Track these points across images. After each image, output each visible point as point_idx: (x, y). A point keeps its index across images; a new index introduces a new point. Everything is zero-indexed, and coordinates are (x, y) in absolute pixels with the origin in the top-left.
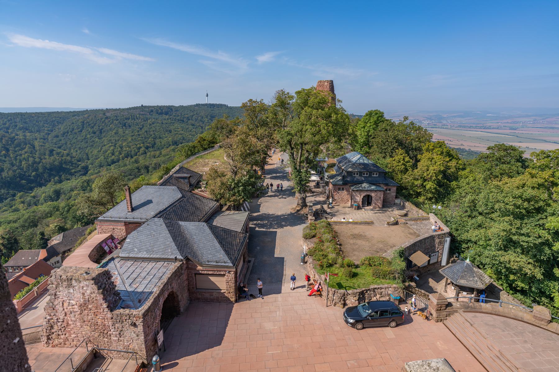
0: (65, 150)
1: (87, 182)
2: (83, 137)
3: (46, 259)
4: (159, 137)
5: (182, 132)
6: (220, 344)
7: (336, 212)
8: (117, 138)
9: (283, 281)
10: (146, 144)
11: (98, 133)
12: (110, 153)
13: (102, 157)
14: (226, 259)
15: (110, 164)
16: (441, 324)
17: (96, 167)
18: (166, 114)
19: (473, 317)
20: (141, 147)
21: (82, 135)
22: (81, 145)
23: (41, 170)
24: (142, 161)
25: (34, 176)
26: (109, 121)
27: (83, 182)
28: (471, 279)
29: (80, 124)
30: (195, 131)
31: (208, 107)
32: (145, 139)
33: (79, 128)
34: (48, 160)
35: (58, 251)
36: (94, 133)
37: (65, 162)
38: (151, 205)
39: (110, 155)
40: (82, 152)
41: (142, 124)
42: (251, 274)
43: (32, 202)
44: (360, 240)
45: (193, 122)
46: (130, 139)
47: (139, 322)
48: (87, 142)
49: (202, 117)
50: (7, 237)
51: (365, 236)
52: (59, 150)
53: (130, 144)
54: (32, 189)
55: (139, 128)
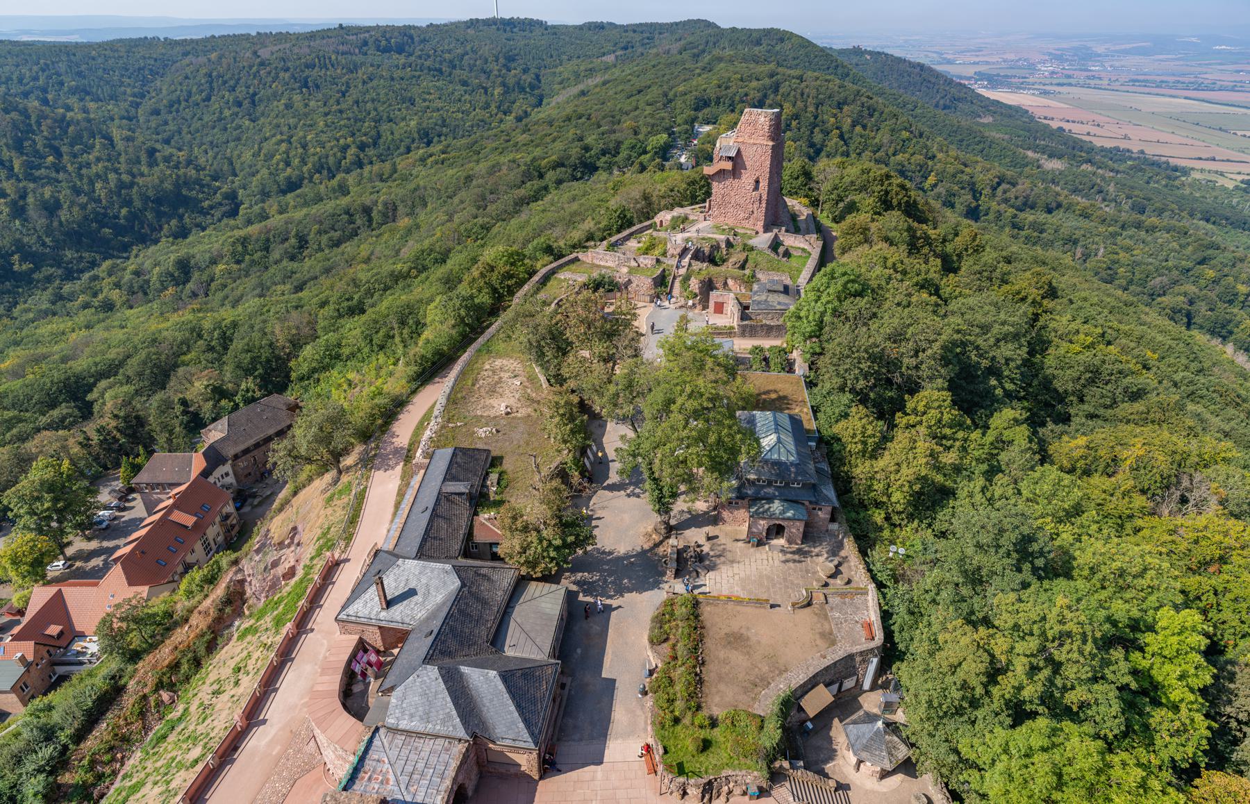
0: (180, 150)
1: (243, 244)
3: (205, 473)
5: (438, 104)
7: (719, 556)
11: (246, 104)
13: (265, 172)
14: (525, 735)
18: (400, 50)
20: (348, 146)
21: (211, 109)
23: (138, 203)
24: (358, 195)
25: (125, 218)
26: (269, 73)
31: (498, 29)
33: (202, 91)
34: (152, 178)
35: (224, 454)
36: (240, 104)
37: (185, 183)
38: (416, 598)
39: (281, 165)
40: (217, 154)
41: (344, 80)
43: (135, 285)
45: (464, 75)
46: (322, 123)
48: (225, 129)
49: (486, 61)
50: (122, 414)
51: (748, 639)
52: (168, 150)
53: (324, 137)
54: (126, 248)
55: (338, 92)
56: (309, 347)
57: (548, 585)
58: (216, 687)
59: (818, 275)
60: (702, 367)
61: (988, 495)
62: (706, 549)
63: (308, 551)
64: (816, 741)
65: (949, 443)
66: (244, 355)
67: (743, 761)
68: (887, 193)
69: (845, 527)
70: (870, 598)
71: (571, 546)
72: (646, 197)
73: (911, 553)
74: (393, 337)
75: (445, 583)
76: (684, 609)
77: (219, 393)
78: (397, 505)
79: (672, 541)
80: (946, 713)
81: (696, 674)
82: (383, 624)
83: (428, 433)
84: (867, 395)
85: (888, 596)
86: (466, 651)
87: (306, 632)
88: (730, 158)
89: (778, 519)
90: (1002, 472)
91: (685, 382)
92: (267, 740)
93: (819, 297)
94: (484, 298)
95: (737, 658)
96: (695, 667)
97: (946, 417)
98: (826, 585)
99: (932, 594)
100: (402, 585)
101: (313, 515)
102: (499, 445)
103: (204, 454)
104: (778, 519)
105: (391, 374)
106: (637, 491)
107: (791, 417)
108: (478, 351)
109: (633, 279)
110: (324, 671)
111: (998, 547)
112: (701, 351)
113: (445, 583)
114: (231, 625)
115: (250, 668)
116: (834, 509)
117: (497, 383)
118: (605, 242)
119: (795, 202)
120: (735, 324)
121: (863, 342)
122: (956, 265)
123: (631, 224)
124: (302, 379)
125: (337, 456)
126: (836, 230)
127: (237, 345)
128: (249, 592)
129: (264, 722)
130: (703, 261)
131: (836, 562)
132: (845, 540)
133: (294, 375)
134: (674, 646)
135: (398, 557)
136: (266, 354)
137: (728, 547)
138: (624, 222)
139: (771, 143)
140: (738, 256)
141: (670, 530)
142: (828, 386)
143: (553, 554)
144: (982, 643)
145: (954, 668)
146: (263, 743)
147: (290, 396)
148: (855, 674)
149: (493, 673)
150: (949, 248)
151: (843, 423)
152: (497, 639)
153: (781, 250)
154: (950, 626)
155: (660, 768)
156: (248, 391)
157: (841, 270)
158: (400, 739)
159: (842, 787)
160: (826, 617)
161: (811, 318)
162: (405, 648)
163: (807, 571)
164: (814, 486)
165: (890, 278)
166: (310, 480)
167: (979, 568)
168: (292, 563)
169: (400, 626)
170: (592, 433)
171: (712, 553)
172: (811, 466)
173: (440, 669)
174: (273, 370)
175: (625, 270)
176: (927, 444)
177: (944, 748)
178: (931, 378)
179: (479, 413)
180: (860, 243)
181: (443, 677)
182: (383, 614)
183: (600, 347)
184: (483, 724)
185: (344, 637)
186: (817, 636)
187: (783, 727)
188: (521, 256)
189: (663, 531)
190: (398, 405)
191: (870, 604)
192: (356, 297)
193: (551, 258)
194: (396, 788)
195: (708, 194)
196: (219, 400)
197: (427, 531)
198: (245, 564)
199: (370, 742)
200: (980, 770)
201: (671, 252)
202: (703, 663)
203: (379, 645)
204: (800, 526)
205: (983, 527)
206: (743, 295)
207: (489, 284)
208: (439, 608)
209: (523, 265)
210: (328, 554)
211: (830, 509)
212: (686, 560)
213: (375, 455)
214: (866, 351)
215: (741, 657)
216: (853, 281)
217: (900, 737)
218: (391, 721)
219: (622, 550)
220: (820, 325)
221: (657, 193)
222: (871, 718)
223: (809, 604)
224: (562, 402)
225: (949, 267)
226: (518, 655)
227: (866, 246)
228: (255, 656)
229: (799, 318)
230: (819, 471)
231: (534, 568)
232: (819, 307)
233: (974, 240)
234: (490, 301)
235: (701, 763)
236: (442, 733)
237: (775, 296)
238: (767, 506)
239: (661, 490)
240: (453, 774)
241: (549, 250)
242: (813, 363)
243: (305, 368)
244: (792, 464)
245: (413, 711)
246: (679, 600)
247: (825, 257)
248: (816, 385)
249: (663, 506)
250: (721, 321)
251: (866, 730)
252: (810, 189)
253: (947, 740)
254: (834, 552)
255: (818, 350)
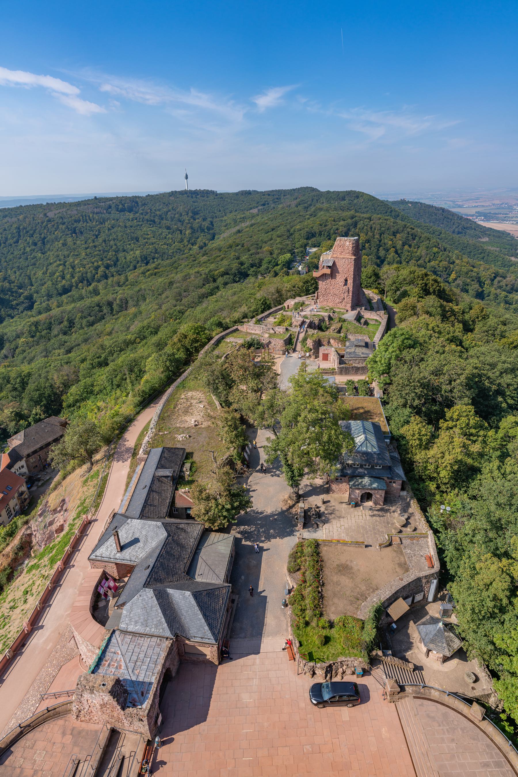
1: (35, 326)
2: (20, 250)
3: (10, 466)
4: (123, 249)
6: (205, 720)
7: (331, 514)
8: (66, 253)
9: (263, 635)
10: (106, 262)
11: (39, 244)
12: (60, 276)
13: (49, 283)
15: (60, 292)
16: (393, 704)
17: (43, 297)
18: (130, 210)
19: (420, 705)
21: (19, 248)
22: (20, 263)
26: (53, 226)
27: (31, 325)
28: (440, 645)
29: (15, 231)
30: (172, 239)
31: (188, 196)
32: (104, 252)
33: (14, 237)
35: (21, 454)
36: (35, 244)
38: (139, 544)
40: (22, 273)
41: (97, 228)
42: (233, 622)
44: (344, 575)
45: (168, 223)
46: (84, 254)
47: (145, 719)
48: (27, 259)
49: (181, 215)
51: (351, 568)
53: (85, 262)
55: (93, 235)
56: (74, 387)
57: (222, 534)
58: (12, 604)
59: (386, 336)
60: (316, 393)
61: (502, 471)
62: (322, 509)
63: (72, 514)
64: (399, 637)
65: (475, 438)
66: (35, 393)
67: (351, 651)
68: (426, 285)
69: (411, 493)
70: (429, 540)
71: (237, 509)
72: (278, 291)
73: (455, 510)
74: (126, 379)
75: (157, 534)
76: (309, 549)
77: (19, 416)
78: (128, 484)
79: (301, 505)
80: (484, 617)
81: (319, 592)
82: (118, 561)
83: (146, 439)
84: (420, 409)
85: (442, 538)
86: (171, 578)
87: (70, 567)
88: (329, 267)
89: (368, 489)
90: (510, 456)
91: (306, 403)
92: (44, 639)
93: (387, 349)
94: (181, 355)
95: (345, 581)
96: (318, 587)
97: (472, 422)
98: (401, 532)
99: (470, 536)
100: (130, 536)
101: (75, 492)
102: (191, 445)
103: (9, 454)
104: (368, 489)
105: (124, 402)
106: (278, 472)
107: (374, 424)
108: (178, 387)
109: (272, 340)
110: (80, 594)
111: (511, 505)
112: (315, 384)
113: (157, 534)
114: (23, 563)
115: (34, 591)
116: (403, 482)
117: (189, 406)
118: (254, 319)
119: (370, 292)
120: (336, 367)
121: (416, 376)
122: (472, 327)
123: (269, 308)
124: (69, 406)
125: (91, 453)
126: (396, 308)
127: (31, 386)
128: (34, 541)
129: (42, 627)
130: (315, 329)
131: (406, 517)
132: (412, 502)
133: (64, 404)
134: (304, 573)
135: (128, 517)
136: (48, 392)
137: (337, 508)
138: (266, 306)
139: (354, 257)
140: (335, 326)
141: (299, 497)
142: (395, 404)
143: (225, 514)
144: (505, 569)
145: (488, 586)
146: (41, 641)
147: (62, 418)
148: (422, 591)
149: (188, 593)
150: (467, 317)
151: (406, 427)
152: (190, 570)
153: (363, 321)
154: (483, 558)
155: (297, 656)
156: (36, 414)
157: (400, 332)
158: (128, 638)
159: (418, 668)
160: (402, 553)
161: (383, 362)
162: (132, 577)
163: (388, 523)
164: (390, 468)
165: (431, 336)
166: (74, 469)
167: (500, 519)
168: (62, 523)
169: (129, 563)
170: (248, 437)
171: (326, 512)
172: (387, 455)
173: (154, 591)
174: (52, 401)
175: (267, 335)
176: (460, 439)
177: (484, 640)
178: (461, 398)
179: (178, 425)
180: (411, 315)
181: (156, 596)
182: (118, 555)
183: (252, 383)
184: (181, 627)
185: (93, 570)
186: (397, 566)
187: (376, 627)
188: (203, 329)
189: (295, 498)
190: (129, 421)
191: (430, 544)
192: (103, 356)
193: (221, 329)
194: (126, 671)
195: (317, 288)
196: (19, 421)
197: (146, 501)
198: (32, 524)
199: (109, 640)
200: (509, 656)
201: (295, 324)
202: (323, 585)
203: (116, 575)
204: (383, 493)
205: (500, 493)
206: (340, 349)
207: (184, 346)
208: (153, 551)
209: (204, 334)
210: (84, 516)
211: (400, 482)
212: (310, 517)
213: (114, 453)
214: (418, 381)
215: (347, 581)
216: (407, 339)
217: (454, 633)
218: (123, 626)
219: (269, 510)
220: (389, 366)
221: (285, 289)
222: (434, 621)
223: (390, 545)
224: (230, 418)
225: (468, 328)
226: (204, 580)
227: (415, 317)
228: (38, 583)
229: (376, 362)
230: (392, 458)
231: (213, 524)
232: (387, 355)
233: (482, 311)
234: (185, 356)
235: (324, 653)
236: (155, 634)
237: (360, 349)
238: (360, 481)
239: (293, 472)
240: (163, 662)
241: (220, 324)
242: (385, 390)
243: (71, 400)
244: (375, 453)
245: (137, 619)
246: (306, 543)
247: (390, 325)
248: (388, 403)
249: (294, 482)
250: (325, 365)
251: (432, 629)
252: (379, 284)
253: (486, 635)
254: (405, 510)
255: (388, 381)
